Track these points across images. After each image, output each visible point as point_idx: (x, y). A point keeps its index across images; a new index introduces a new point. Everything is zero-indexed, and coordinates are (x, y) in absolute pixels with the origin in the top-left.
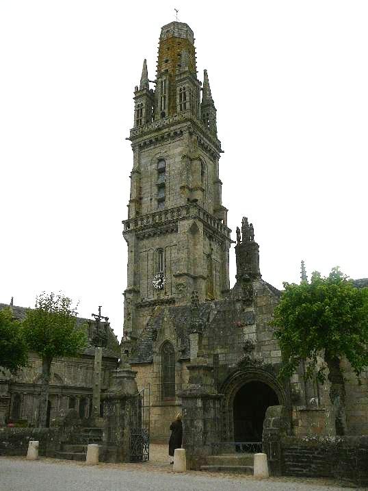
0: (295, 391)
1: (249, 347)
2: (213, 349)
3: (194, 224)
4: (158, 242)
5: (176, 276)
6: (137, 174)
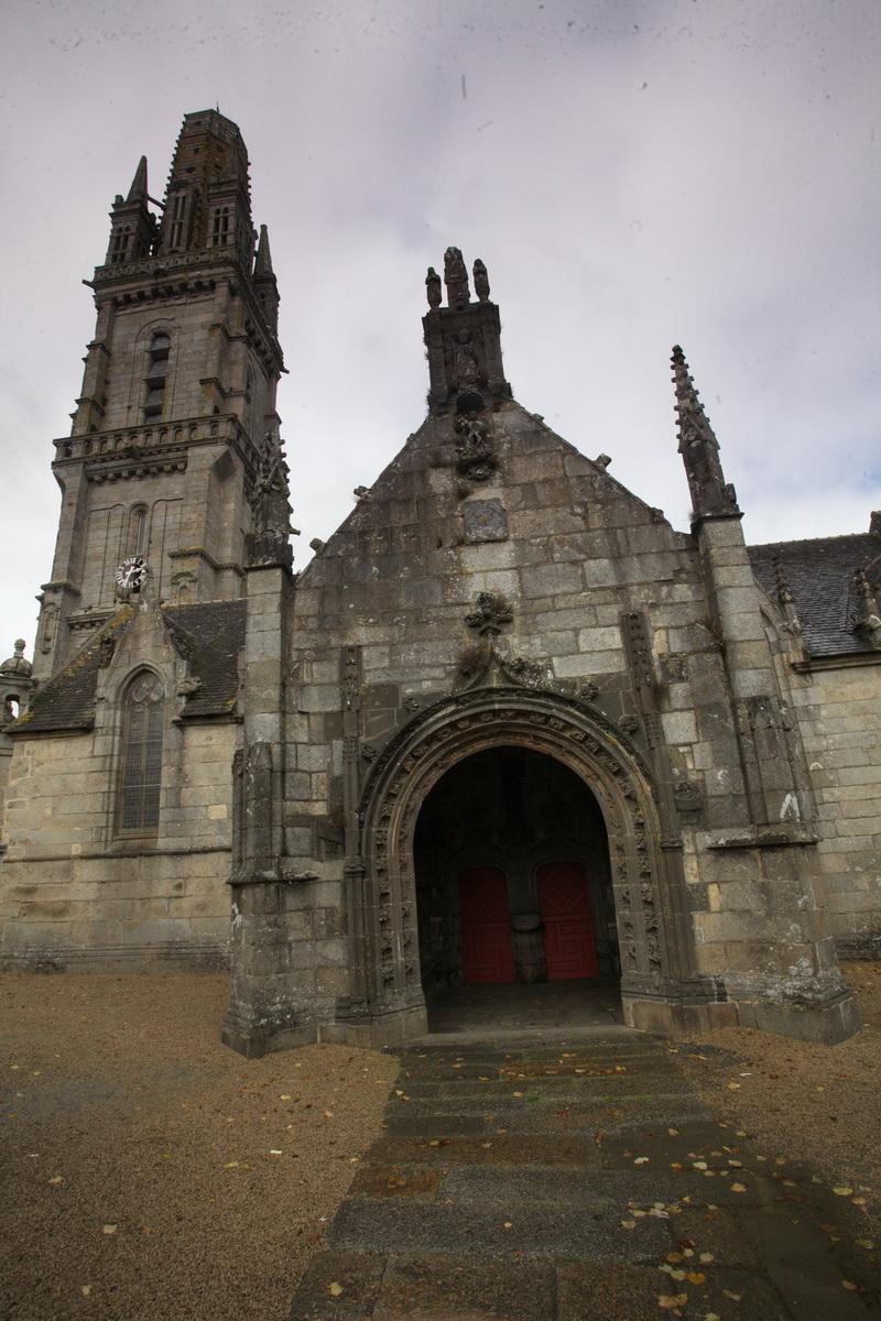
0: (684, 773)
1: (492, 616)
2: (341, 627)
3: (227, 455)
4: (137, 490)
5: (173, 556)
6: (101, 354)
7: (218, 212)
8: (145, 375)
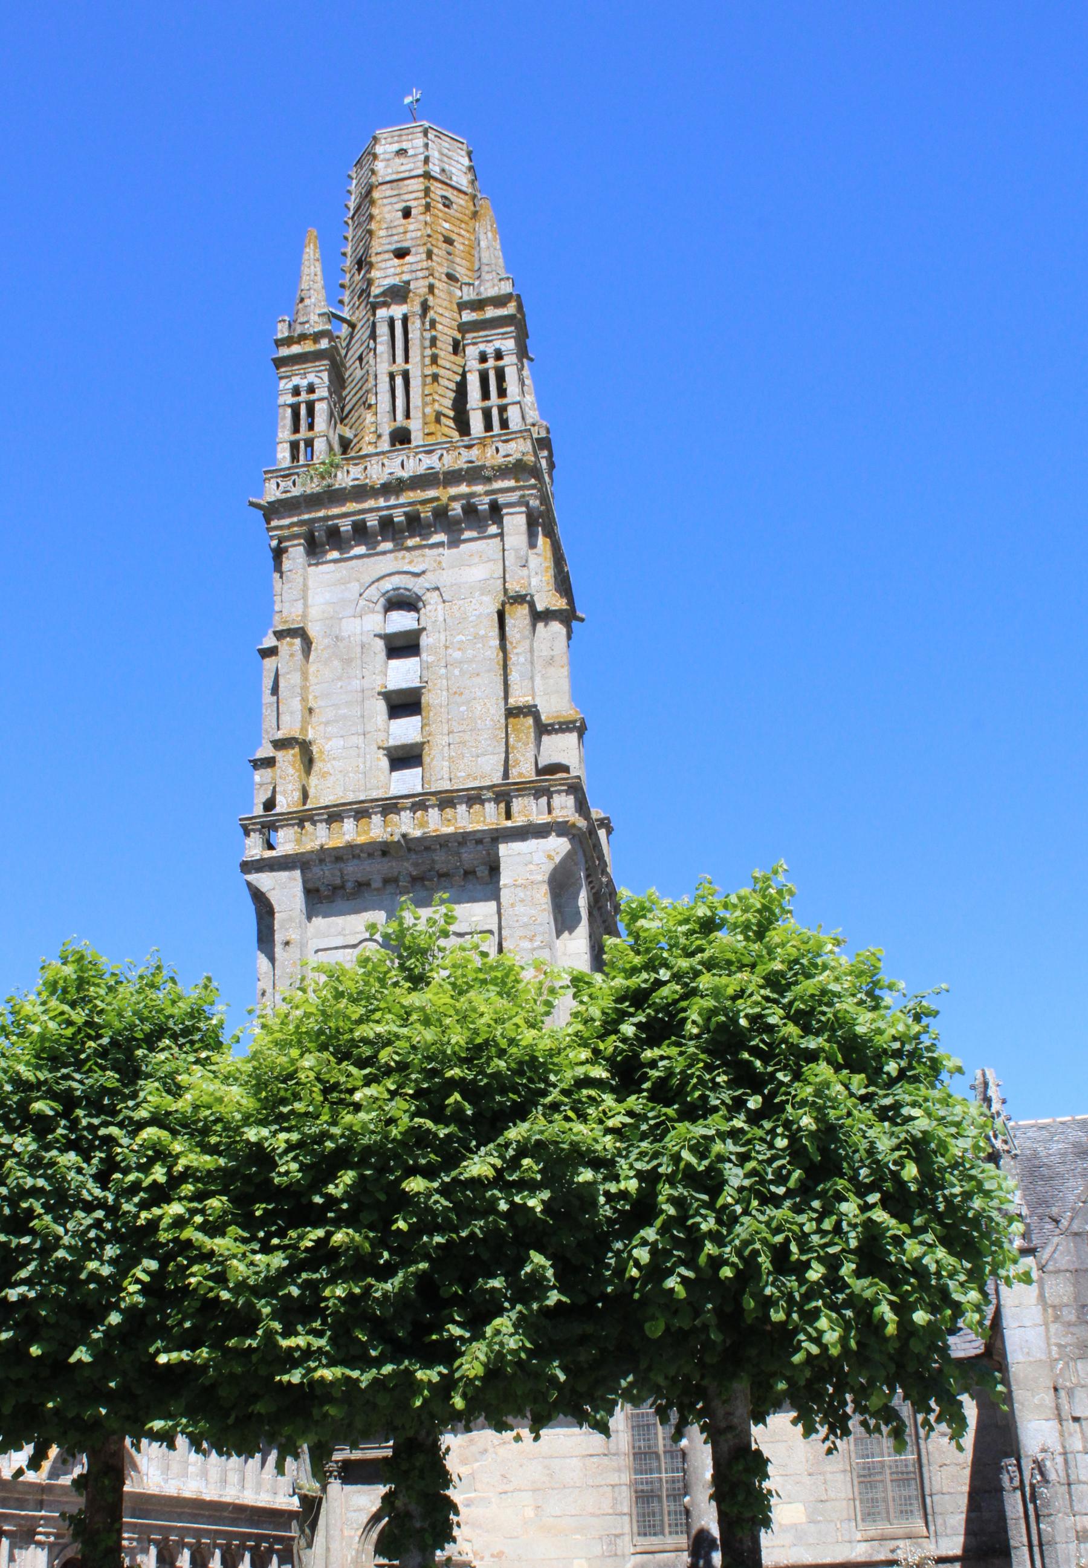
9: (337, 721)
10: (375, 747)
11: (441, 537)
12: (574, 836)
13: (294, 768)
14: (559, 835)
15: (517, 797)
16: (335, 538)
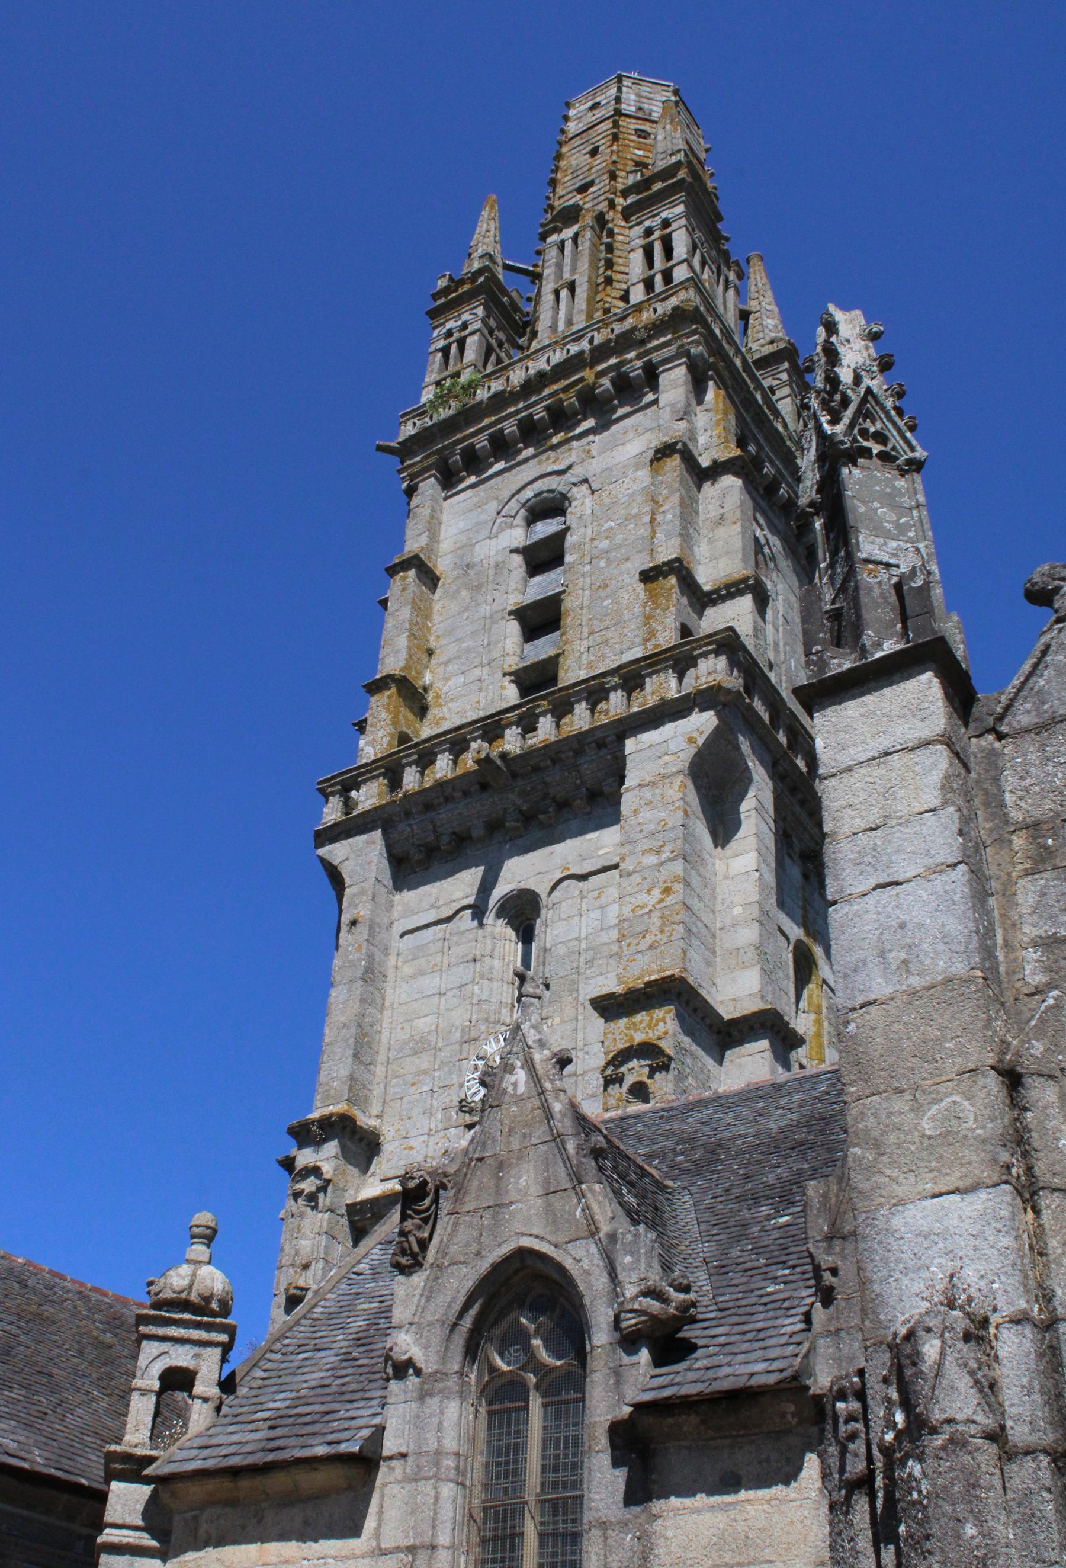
7: (649, 232)
8: (515, 600)
9: (459, 657)
10: (500, 674)
11: (590, 423)
12: (725, 705)
13: (388, 710)
14: (702, 710)
15: (650, 675)
16: (474, 462)
